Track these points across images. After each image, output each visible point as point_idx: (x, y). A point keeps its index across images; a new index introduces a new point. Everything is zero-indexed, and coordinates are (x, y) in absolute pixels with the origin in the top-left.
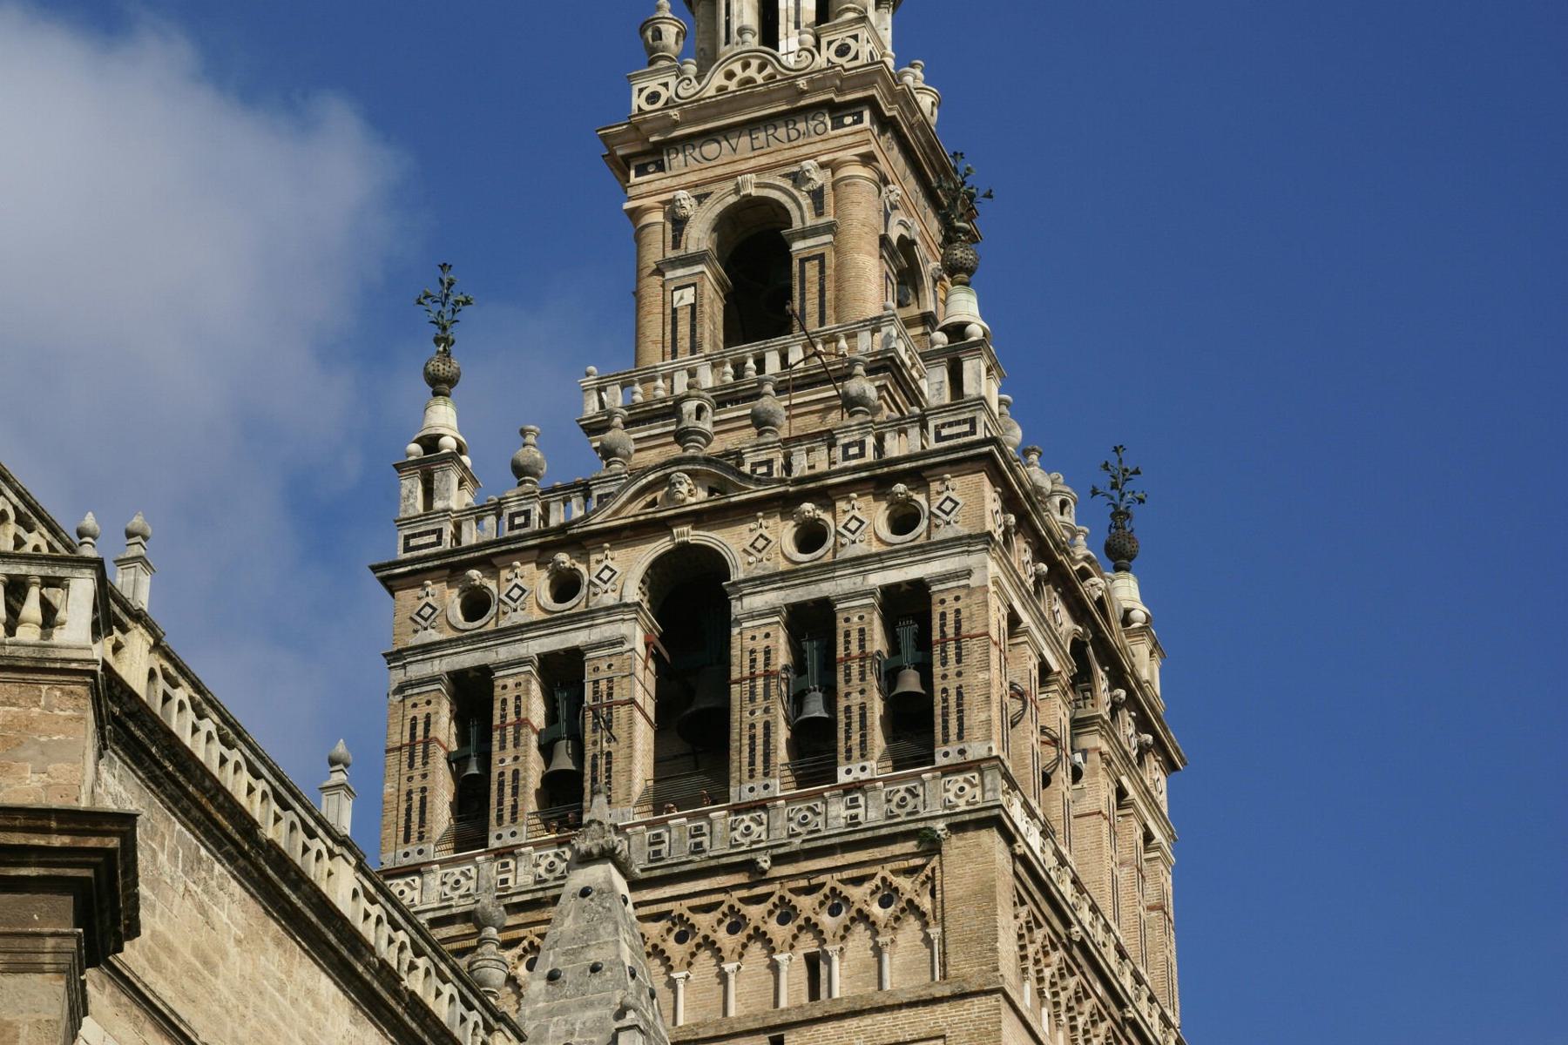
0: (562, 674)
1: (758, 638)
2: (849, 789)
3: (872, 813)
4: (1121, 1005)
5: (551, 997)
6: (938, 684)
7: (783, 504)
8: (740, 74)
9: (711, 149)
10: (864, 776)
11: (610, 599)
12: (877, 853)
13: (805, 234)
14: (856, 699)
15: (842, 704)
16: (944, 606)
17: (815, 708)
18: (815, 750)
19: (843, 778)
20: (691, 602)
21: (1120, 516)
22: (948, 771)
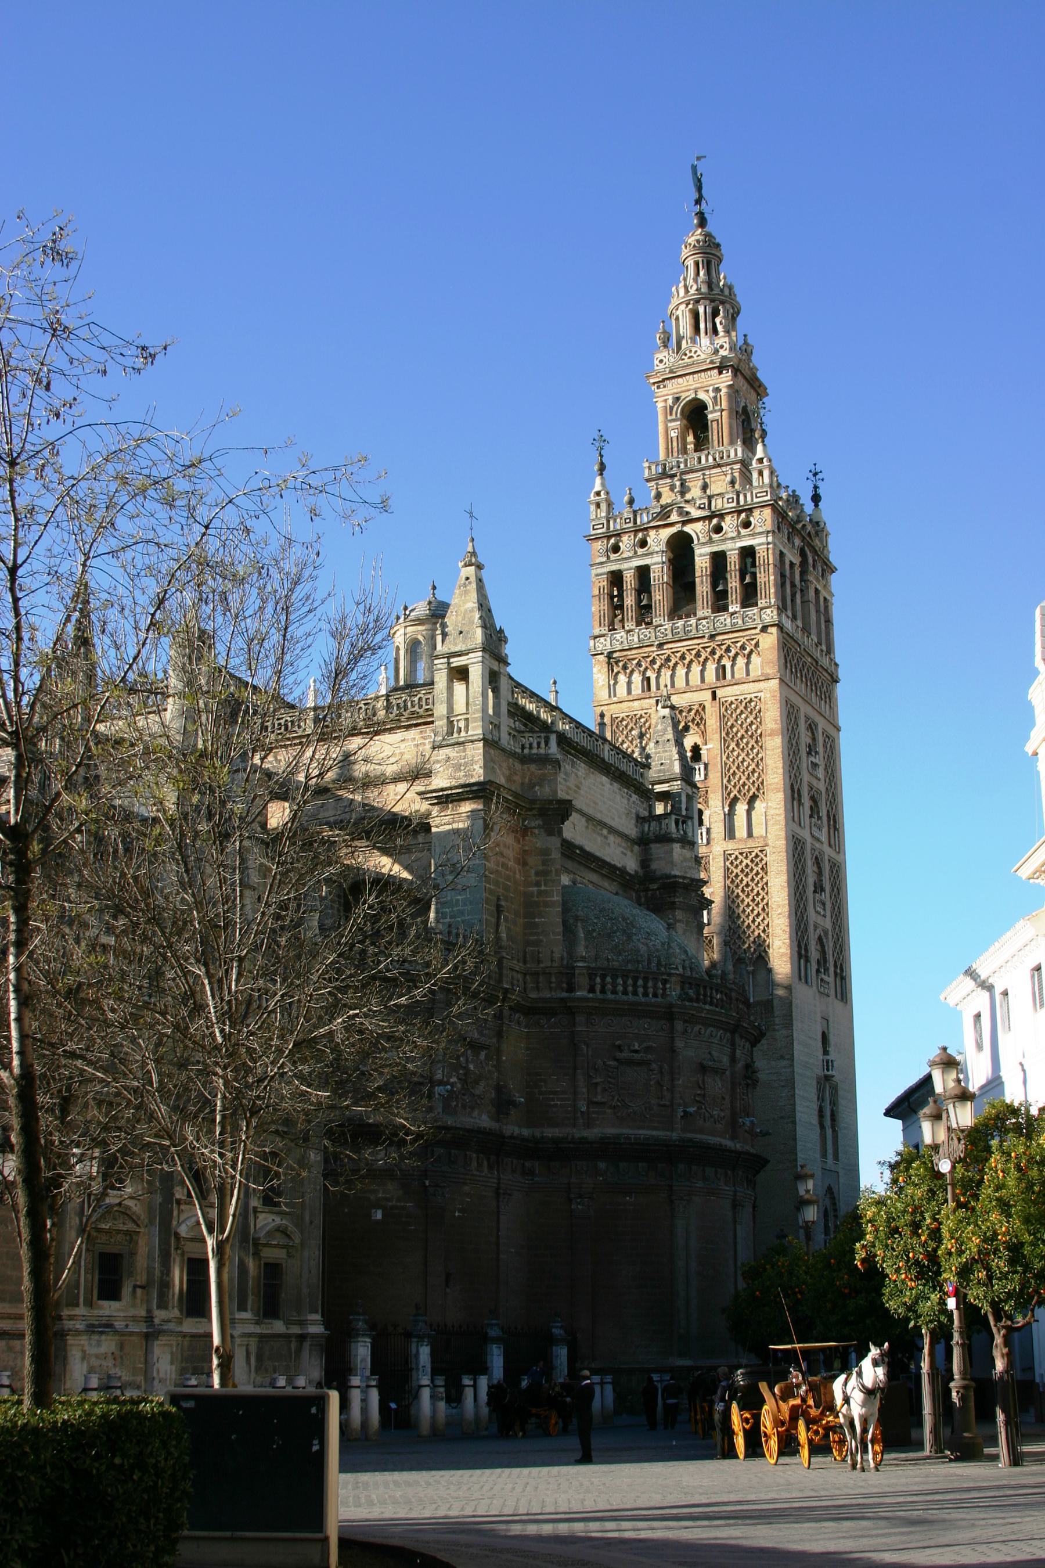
0: (643, 572)
1: (702, 561)
2: (732, 614)
4: (817, 662)
5: (656, 748)
6: (758, 580)
7: (709, 518)
8: (689, 355)
10: (738, 609)
11: (657, 549)
12: (741, 634)
13: (712, 412)
15: (730, 585)
16: (761, 553)
17: (720, 588)
19: (731, 610)
20: (681, 549)
21: (816, 487)
22: (762, 609)
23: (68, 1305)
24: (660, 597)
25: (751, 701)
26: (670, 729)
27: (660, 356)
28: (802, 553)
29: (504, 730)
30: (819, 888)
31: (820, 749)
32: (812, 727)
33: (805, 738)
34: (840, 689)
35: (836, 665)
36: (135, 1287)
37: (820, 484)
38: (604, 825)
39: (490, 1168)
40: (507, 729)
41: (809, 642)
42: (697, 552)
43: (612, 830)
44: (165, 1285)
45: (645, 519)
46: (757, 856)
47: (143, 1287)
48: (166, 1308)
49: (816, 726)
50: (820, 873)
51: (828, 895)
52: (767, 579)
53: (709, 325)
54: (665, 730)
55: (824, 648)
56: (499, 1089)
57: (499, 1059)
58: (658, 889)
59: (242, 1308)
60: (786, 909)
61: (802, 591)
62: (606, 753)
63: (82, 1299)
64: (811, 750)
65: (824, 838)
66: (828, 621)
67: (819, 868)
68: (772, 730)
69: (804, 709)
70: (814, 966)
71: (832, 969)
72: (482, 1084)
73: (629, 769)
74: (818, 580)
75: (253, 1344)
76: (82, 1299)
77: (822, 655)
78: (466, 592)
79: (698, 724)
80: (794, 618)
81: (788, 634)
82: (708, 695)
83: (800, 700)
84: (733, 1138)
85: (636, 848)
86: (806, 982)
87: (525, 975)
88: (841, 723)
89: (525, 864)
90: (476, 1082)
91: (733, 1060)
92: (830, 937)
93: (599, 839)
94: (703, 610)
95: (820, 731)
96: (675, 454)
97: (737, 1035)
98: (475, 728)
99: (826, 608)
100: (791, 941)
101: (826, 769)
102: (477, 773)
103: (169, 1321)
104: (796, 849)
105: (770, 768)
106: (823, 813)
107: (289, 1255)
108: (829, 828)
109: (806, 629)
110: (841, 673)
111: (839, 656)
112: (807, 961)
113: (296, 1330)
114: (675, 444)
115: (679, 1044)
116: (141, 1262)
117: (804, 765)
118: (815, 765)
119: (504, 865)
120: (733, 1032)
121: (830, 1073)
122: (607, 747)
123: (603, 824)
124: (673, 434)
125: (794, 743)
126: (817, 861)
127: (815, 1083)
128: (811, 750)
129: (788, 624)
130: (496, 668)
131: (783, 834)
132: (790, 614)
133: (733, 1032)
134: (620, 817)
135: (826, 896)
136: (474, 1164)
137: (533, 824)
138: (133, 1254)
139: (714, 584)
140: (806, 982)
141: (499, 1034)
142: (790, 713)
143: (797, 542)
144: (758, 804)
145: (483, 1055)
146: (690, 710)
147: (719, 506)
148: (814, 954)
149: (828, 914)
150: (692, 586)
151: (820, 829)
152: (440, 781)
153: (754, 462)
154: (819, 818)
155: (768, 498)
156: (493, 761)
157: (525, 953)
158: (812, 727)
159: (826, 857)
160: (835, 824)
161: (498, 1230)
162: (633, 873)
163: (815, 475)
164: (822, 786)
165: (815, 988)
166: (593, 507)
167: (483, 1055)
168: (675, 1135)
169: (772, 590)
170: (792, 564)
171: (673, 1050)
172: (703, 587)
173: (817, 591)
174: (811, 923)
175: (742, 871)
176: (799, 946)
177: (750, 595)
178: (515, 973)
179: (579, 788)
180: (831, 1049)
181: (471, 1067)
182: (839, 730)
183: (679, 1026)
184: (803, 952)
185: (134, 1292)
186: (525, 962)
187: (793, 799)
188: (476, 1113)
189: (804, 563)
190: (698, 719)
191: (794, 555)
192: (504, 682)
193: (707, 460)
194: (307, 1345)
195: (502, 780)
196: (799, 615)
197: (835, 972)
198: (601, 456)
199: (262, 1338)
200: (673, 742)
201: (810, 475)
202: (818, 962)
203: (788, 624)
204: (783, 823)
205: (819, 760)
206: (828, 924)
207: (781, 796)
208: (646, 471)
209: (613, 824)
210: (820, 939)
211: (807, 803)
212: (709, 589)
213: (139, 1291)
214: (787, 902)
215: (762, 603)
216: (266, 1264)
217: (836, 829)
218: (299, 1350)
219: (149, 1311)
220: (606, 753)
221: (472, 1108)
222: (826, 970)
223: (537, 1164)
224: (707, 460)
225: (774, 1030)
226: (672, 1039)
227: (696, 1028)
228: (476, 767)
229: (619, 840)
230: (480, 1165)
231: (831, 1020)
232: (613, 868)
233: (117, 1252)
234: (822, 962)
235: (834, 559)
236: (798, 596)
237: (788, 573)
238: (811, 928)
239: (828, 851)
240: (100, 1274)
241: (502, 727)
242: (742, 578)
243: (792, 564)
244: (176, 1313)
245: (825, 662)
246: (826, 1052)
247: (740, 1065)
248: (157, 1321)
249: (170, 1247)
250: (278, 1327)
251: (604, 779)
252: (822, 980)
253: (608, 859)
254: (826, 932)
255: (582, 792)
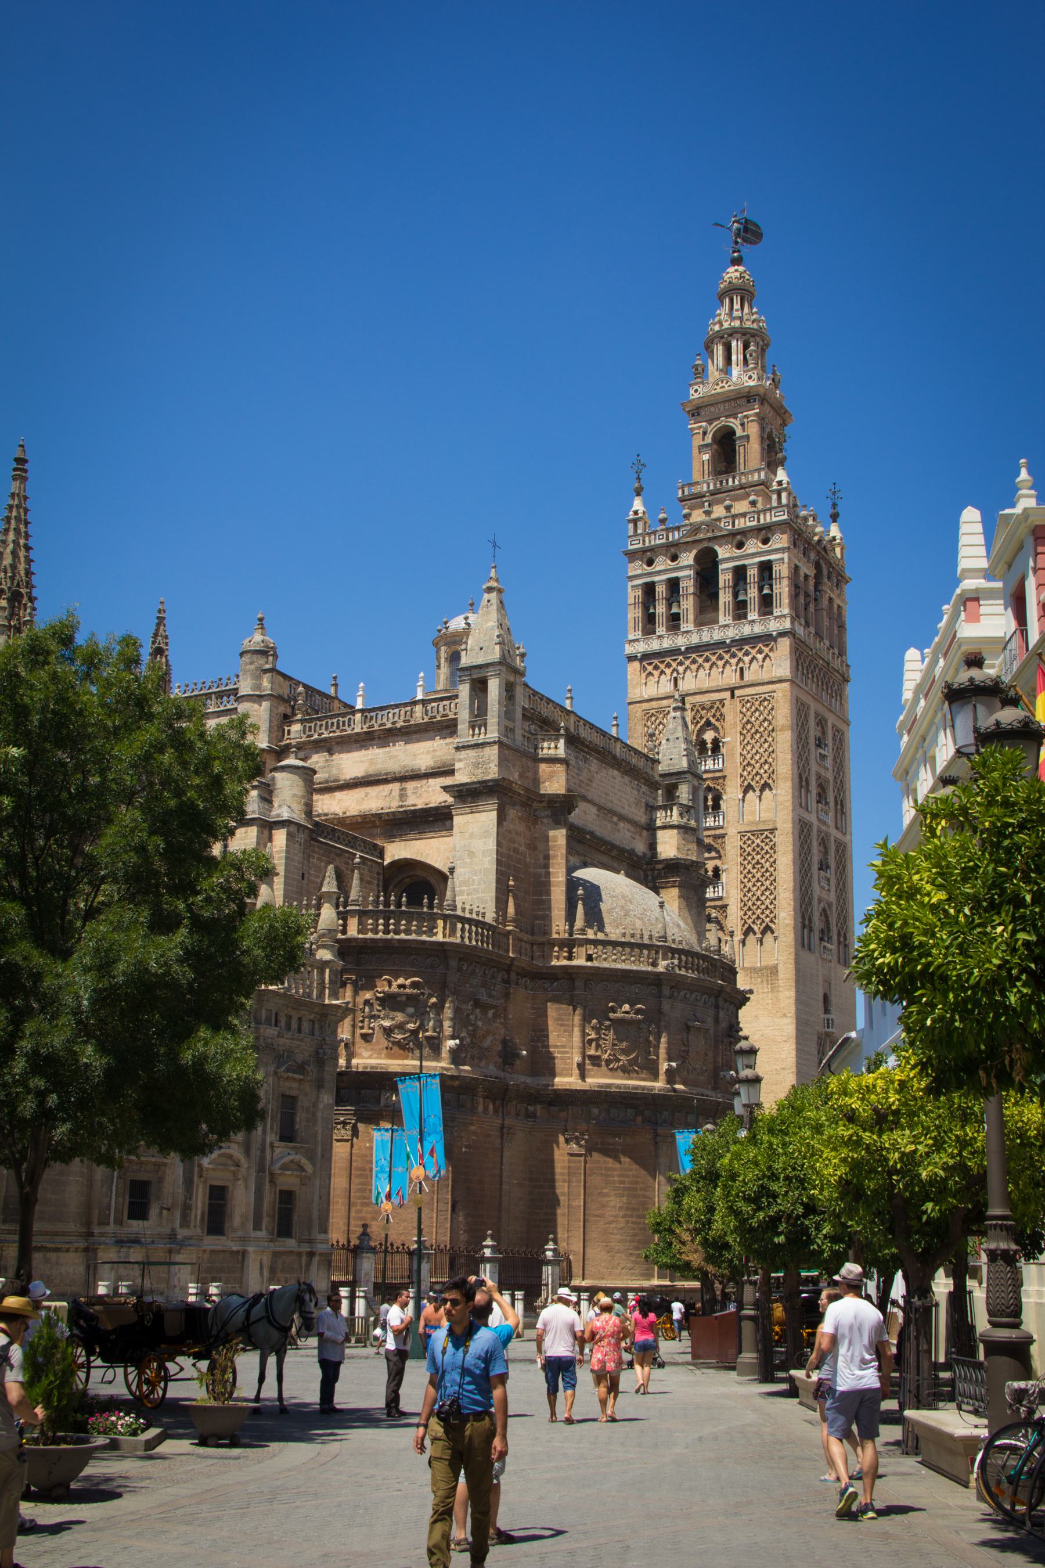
3: (758, 629)
4: (828, 664)
6: (775, 591)
8: (721, 385)
9: (712, 409)
11: (686, 563)
14: (752, 595)
16: (776, 568)
18: (740, 609)
19: (749, 618)
21: (834, 506)
23: (99, 1224)
24: (688, 605)
25: (765, 699)
26: (680, 728)
27: (696, 387)
28: (817, 566)
29: (519, 732)
30: (823, 866)
31: (829, 741)
32: (821, 722)
33: (813, 731)
34: (849, 689)
35: (848, 666)
36: (162, 1208)
37: (839, 502)
38: (614, 813)
39: (496, 1111)
40: (522, 732)
41: (822, 646)
42: (721, 567)
43: (622, 818)
44: (187, 1208)
45: (677, 536)
46: (767, 837)
47: (169, 1210)
48: (188, 1227)
49: (826, 721)
50: (826, 852)
51: (833, 872)
52: (782, 590)
53: (741, 357)
54: (676, 729)
55: (836, 651)
56: (505, 1042)
57: (506, 1017)
58: (663, 868)
59: (257, 1227)
60: (791, 884)
61: (816, 600)
62: (618, 749)
63: (112, 1219)
64: (820, 743)
65: (830, 821)
66: (842, 627)
67: (825, 848)
68: (783, 726)
69: (813, 706)
70: (816, 935)
71: (835, 937)
72: (489, 1039)
73: (641, 763)
74: (832, 590)
75: (266, 1259)
76: (112, 1219)
77: (833, 658)
78: (488, 613)
79: (718, 720)
80: (807, 625)
81: (800, 640)
82: (727, 694)
83: (811, 699)
84: (714, 1089)
85: (645, 832)
86: (810, 949)
87: (532, 945)
88: (851, 716)
89: (535, 849)
90: (484, 1037)
91: (717, 1020)
92: (834, 909)
93: (609, 826)
94: (724, 618)
95: (830, 725)
96: (706, 476)
97: (721, 999)
98: (492, 732)
99: (840, 614)
100: (795, 913)
101: (834, 759)
102: (492, 772)
103: (190, 1238)
104: (803, 831)
105: (780, 759)
106: (831, 799)
107: (303, 1184)
108: (836, 813)
109: (818, 634)
110: (852, 674)
111: (851, 657)
112: (811, 930)
113: (305, 1248)
114: (706, 467)
115: (666, 1006)
116: (168, 1187)
117: (813, 757)
118: (823, 757)
119: (515, 850)
120: (717, 997)
121: (830, 1030)
122: (619, 745)
123: (612, 812)
124: (706, 457)
125: (803, 736)
126: (824, 842)
127: (815, 1038)
128: (820, 743)
129: (800, 631)
130: (512, 679)
131: (790, 818)
132: (803, 621)
133: (717, 997)
134: (629, 806)
135: (831, 874)
136: (481, 1108)
137: (543, 814)
138: (161, 1180)
139: (735, 595)
140: (810, 949)
141: (507, 996)
142: (800, 711)
143: (813, 555)
144: (767, 792)
145: (490, 1013)
146: (712, 707)
147: (742, 526)
148: (817, 923)
149: (833, 889)
150: (715, 596)
151: (826, 813)
152: (461, 778)
153: (774, 483)
154: (827, 803)
155: (785, 517)
156: (508, 761)
157: (533, 926)
158: (821, 722)
159: (832, 839)
160: (841, 808)
161: (502, 1164)
162: (640, 854)
163: (834, 493)
164: (830, 775)
165: (817, 954)
166: (631, 526)
167: (490, 1013)
168: (659, 1085)
169: (787, 601)
170: (806, 577)
171: (660, 1012)
172: (725, 598)
173: (831, 599)
174: (816, 897)
175: (754, 850)
176: (803, 918)
177: (767, 603)
178: (523, 944)
179: (591, 781)
180: (833, 1009)
181: (480, 1023)
182: (848, 725)
183: (666, 991)
184: (807, 922)
185: (161, 1213)
186: (533, 934)
187: (801, 787)
188: (483, 1064)
189: (818, 576)
190: (718, 714)
191: (808, 569)
192: (519, 691)
193: (734, 482)
194: (316, 1259)
195: (515, 776)
196: (812, 621)
197: (839, 943)
198: (639, 479)
199: (276, 1255)
200: (681, 739)
201: (830, 494)
202: (822, 931)
203: (800, 631)
204: (790, 808)
205: (828, 752)
206: (832, 897)
207: (789, 784)
208: (680, 492)
209: (624, 812)
210: (824, 910)
211: (814, 790)
212: (731, 599)
213: (165, 1212)
214: (792, 878)
215: (777, 612)
216: (281, 1191)
217: (843, 813)
218: (308, 1265)
219: (173, 1230)
220: (618, 750)
221: (480, 1059)
222: (830, 939)
223: (539, 1107)
224: (734, 482)
225: (778, 991)
226: (660, 1002)
227: (682, 993)
228: (492, 765)
229: (628, 826)
230: (486, 1109)
231: (833, 983)
232: (622, 851)
233: (145, 1178)
234: (825, 934)
235: (848, 573)
236: (812, 606)
237: (802, 585)
238: (815, 902)
239: (834, 833)
240: (130, 1197)
241: (517, 731)
242: (761, 589)
243: (806, 577)
244: (198, 1230)
245: (836, 664)
246: (827, 1011)
247: (724, 1025)
248: (179, 1237)
249: (193, 1174)
250: (291, 1243)
251: (616, 773)
252: (825, 947)
253: (618, 843)
254: (830, 905)
255: (594, 785)
